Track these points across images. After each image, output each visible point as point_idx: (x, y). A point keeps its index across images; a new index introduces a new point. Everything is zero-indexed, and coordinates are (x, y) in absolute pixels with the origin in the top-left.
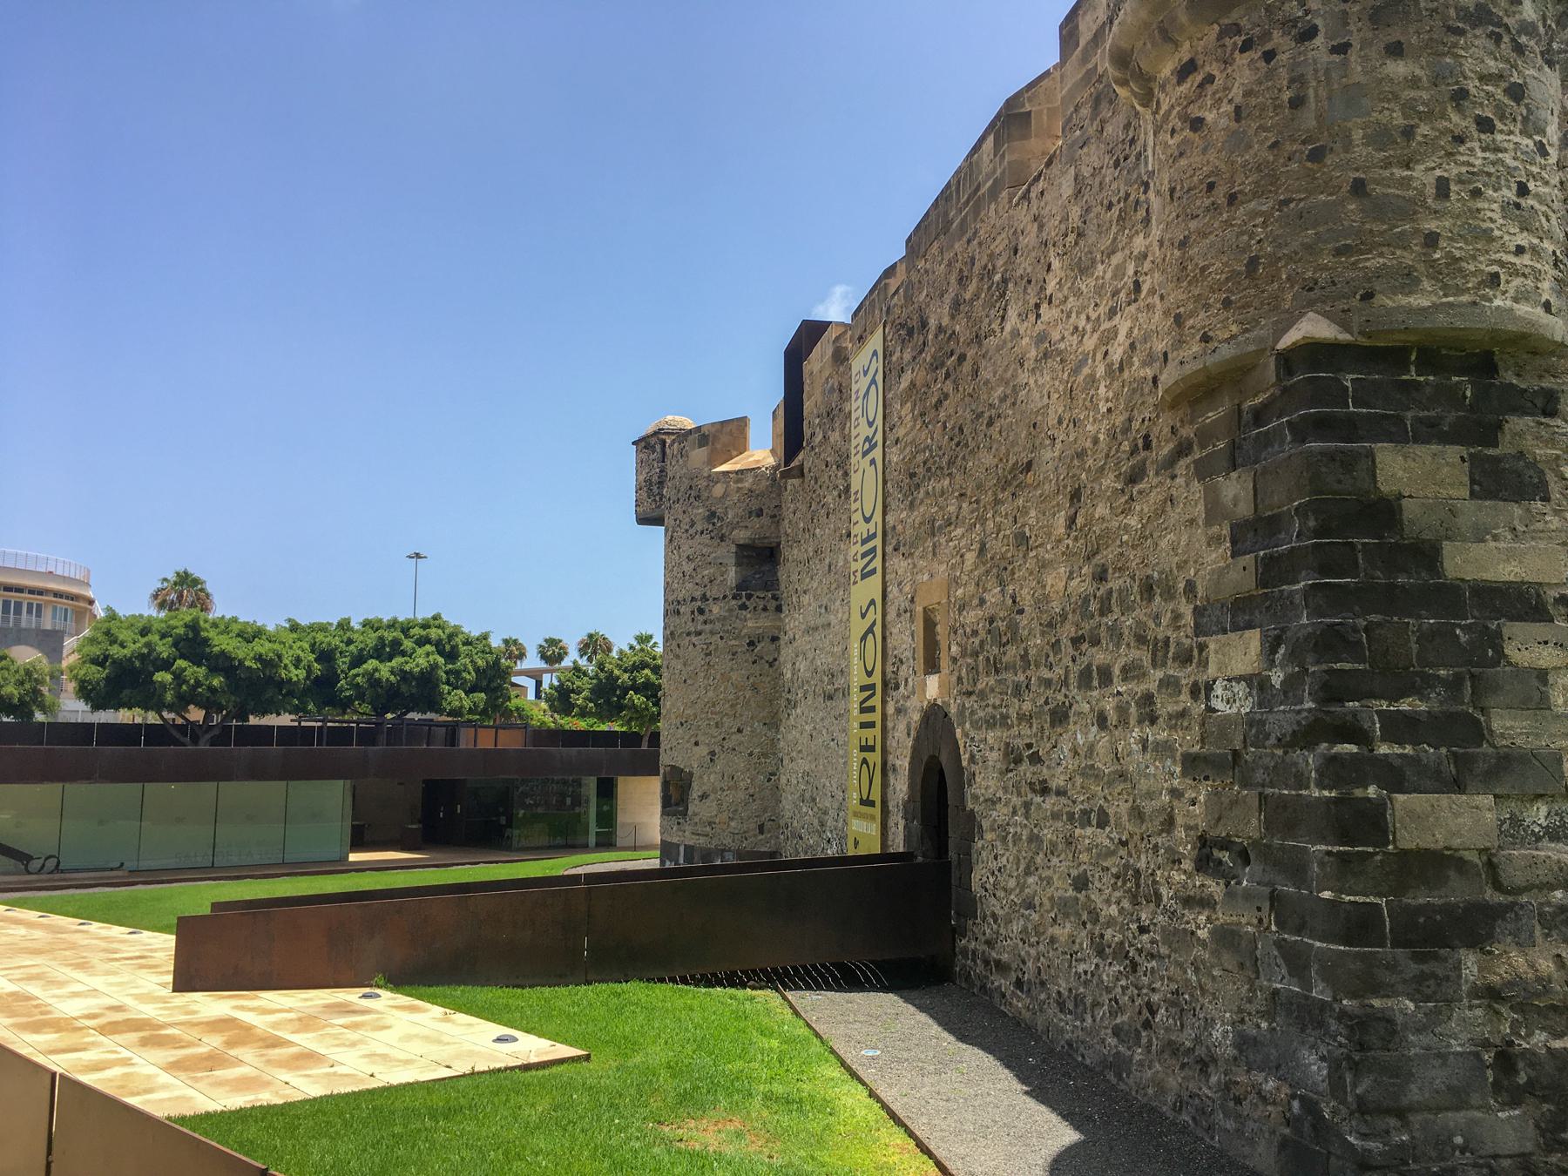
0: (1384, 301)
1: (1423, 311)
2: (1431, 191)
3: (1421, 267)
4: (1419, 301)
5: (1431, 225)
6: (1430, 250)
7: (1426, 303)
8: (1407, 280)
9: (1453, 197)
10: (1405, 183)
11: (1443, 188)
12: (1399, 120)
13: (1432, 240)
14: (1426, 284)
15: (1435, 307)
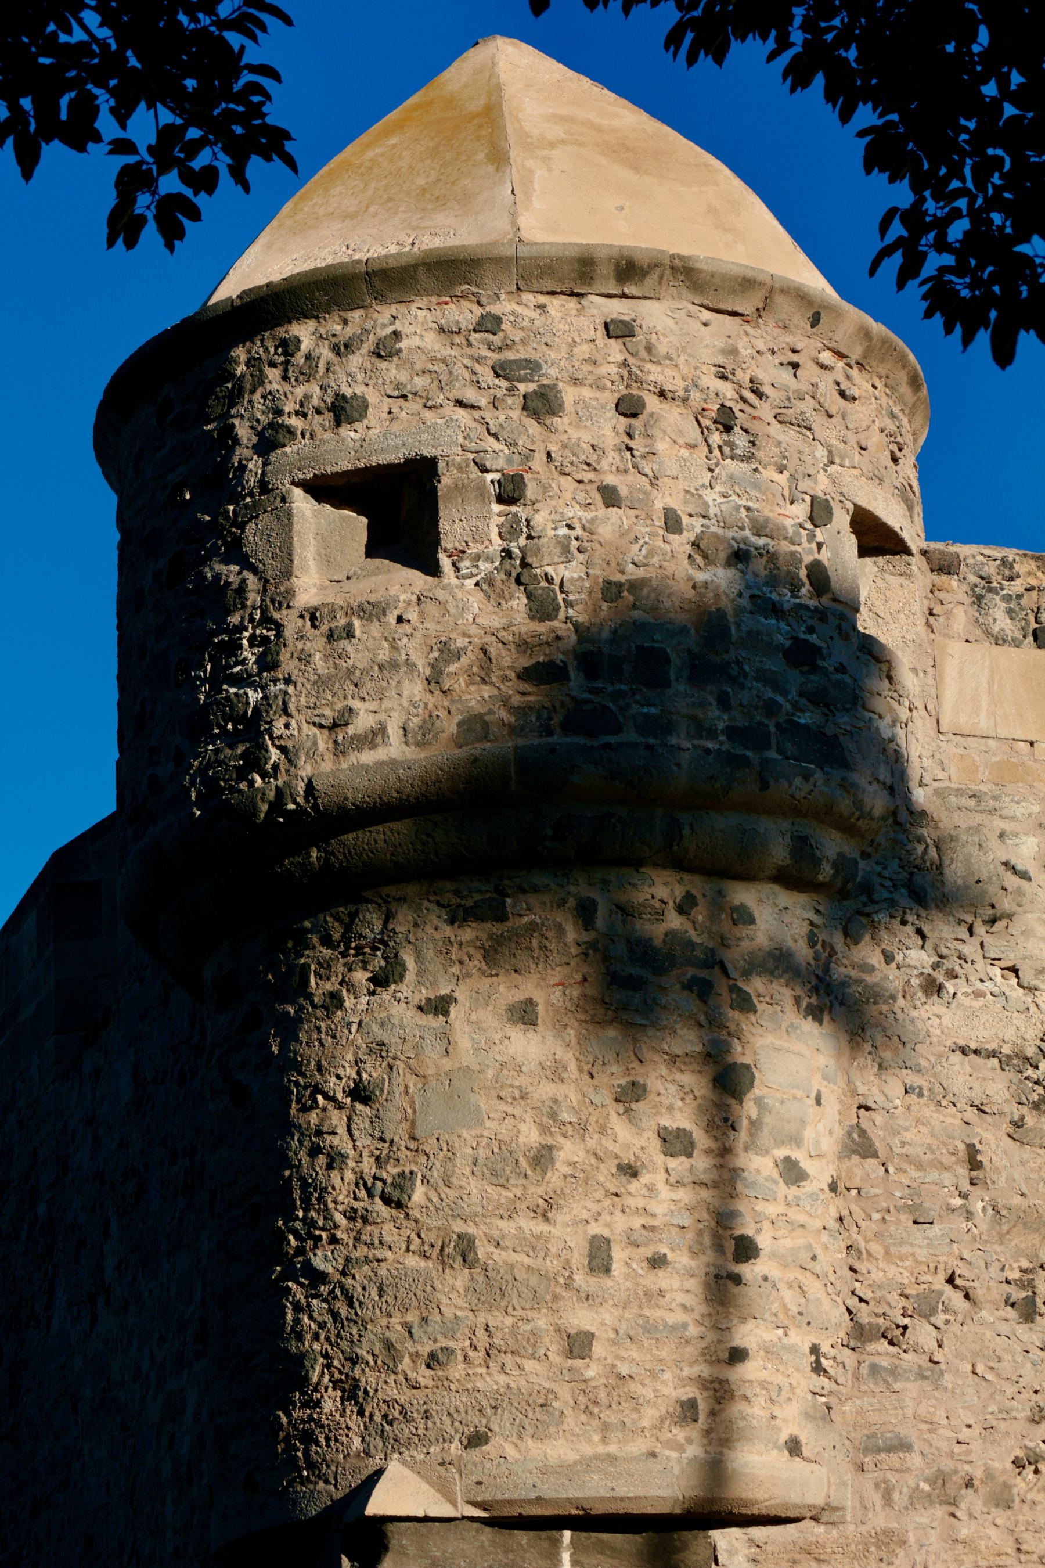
0: (501, 1445)
1: (568, 1471)
2: (579, 1259)
3: (564, 1391)
4: (559, 1450)
5: (580, 1319)
6: (578, 1363)
7: (572, 1456)
8: (538, 1412)
9: (617, 1268)
10: (535, 1245)
11: (599, 1256)
12: (530, 1136)
13: (578, 1345)
14: (572, 1421)
15: (587, 1463)
